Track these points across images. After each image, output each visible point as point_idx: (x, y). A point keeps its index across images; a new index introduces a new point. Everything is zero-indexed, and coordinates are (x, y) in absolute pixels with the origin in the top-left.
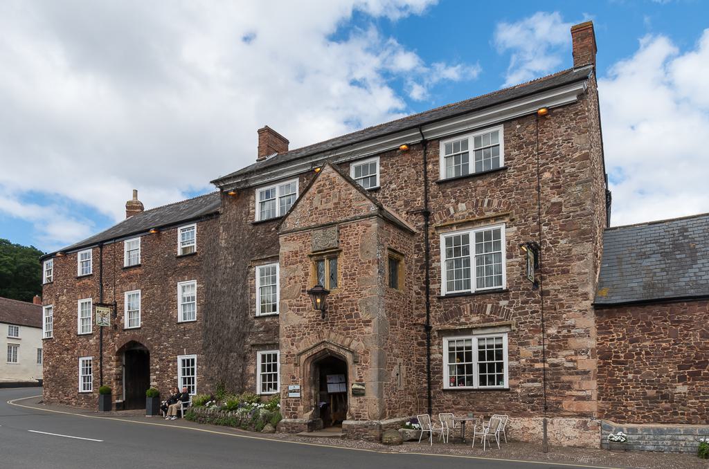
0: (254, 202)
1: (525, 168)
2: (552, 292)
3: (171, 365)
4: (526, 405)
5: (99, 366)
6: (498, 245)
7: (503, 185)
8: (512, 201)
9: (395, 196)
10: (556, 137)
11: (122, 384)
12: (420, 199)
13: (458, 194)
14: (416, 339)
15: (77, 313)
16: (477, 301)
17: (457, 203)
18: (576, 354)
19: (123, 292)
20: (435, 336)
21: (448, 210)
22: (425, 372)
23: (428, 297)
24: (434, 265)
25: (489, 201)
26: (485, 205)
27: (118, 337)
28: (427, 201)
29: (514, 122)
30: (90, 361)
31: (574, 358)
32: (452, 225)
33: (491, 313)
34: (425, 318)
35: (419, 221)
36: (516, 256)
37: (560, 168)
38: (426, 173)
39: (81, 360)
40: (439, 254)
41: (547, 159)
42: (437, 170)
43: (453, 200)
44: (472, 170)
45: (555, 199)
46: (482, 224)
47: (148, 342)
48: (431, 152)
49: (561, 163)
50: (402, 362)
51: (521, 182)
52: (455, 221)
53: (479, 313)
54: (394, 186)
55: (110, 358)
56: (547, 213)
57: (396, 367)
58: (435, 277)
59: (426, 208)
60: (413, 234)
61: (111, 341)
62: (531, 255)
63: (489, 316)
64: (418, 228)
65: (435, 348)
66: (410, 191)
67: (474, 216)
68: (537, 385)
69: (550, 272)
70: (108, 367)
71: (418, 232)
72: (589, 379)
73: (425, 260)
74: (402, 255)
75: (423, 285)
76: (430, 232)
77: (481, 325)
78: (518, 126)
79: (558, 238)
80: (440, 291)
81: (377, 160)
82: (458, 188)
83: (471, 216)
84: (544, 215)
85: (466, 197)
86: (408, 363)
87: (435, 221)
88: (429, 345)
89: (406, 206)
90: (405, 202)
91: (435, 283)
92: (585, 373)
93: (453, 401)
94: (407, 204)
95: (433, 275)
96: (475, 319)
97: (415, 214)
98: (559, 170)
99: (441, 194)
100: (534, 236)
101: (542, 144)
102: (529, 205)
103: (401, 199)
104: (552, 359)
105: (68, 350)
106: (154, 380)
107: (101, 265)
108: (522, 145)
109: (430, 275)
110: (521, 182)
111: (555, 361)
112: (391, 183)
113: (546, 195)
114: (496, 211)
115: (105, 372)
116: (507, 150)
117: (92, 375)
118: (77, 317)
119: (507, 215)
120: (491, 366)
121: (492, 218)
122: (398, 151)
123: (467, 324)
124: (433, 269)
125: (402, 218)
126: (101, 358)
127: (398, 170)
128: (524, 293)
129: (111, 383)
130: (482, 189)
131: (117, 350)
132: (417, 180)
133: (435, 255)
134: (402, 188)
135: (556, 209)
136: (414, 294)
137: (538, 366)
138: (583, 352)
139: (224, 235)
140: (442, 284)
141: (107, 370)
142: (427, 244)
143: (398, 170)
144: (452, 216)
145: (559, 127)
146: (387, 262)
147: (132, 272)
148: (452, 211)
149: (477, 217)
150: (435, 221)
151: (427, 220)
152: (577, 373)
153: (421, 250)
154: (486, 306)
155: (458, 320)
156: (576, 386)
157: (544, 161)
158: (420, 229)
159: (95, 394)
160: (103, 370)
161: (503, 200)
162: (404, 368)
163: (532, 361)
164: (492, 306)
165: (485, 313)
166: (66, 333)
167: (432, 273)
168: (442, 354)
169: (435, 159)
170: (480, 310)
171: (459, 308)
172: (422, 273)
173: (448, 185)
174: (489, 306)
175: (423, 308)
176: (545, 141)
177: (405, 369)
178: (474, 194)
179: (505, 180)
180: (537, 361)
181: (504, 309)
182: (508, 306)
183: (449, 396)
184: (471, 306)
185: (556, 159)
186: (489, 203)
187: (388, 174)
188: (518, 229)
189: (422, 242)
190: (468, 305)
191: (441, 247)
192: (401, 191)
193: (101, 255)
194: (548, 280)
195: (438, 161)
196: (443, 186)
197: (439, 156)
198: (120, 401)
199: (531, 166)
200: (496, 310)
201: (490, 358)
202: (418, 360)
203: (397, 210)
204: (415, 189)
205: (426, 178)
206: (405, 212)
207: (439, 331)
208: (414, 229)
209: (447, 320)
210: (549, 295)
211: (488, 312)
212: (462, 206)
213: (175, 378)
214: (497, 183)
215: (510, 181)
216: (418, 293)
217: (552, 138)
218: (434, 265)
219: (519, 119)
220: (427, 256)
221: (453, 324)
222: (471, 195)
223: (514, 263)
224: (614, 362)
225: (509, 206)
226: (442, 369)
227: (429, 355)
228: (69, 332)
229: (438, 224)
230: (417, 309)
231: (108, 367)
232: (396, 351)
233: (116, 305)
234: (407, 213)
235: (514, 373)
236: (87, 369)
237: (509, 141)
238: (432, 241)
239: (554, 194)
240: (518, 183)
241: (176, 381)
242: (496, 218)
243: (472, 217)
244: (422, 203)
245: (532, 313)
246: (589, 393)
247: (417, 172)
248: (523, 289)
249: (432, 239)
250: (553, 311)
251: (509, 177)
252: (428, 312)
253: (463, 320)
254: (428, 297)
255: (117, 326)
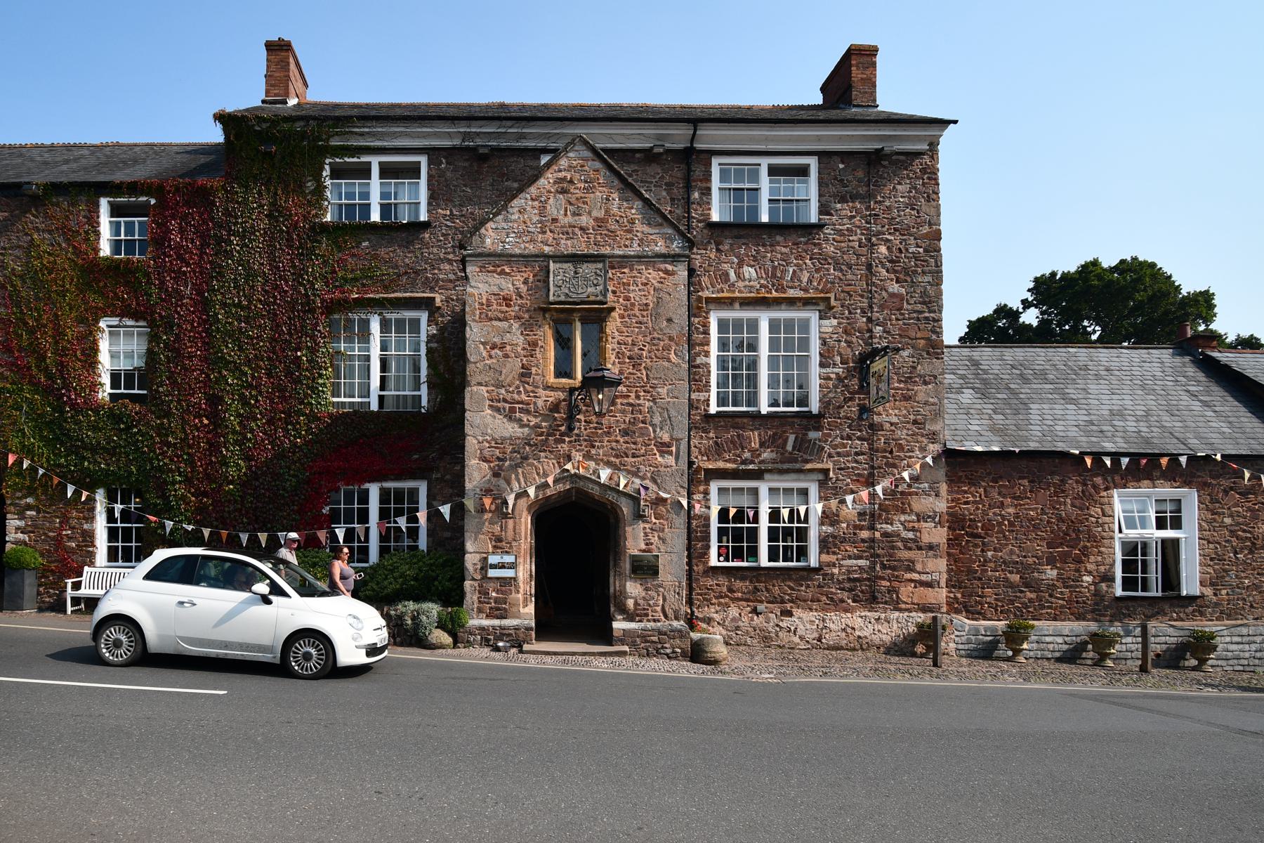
18: (919, 521)
31: (916, 525)
33: (794, 448)
46: (783, 307)
63: (791, 453)
68: (862, 562)
72: (935, 556)
77: (779, 466)
92: (931, 547)
104: (884, 526)
111: (889, 528)
137: (865, 534)
138: (929, 517)
149: (774, 294)
152: (920, 548)
156: (919, 567)
163: (856, 527)
164: (796, 438)
174: (792, 438)
181: (815, 443)
183: (723, 580)
211: (789, 448)
224: (967, 533)
235: (825, 545)
245: (857, 454)
246: (935, 576)
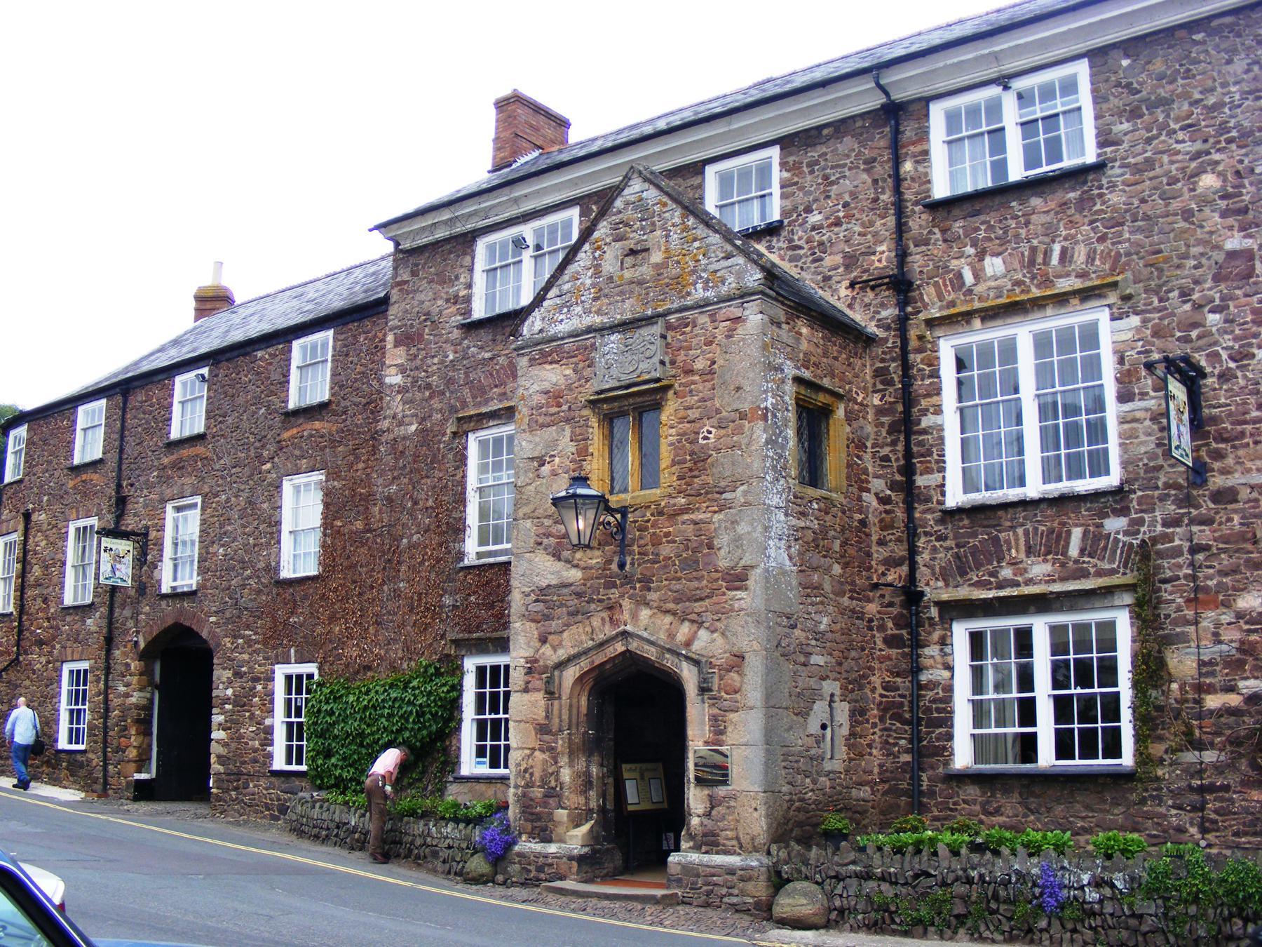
0: (471, 270)
1: (1149, 164)
2: (1244, 494)
3: (259, 687)
4: (1186, 817)
5: (102, 685)
6: (1093, 368)
7: (1098, 207)
8: (1122, 248)
9: (821, 244)
10: (1224, 85)
11: (151, 734)
12: (884, 248)
13: (982, 234)
14: (882, 628)
15: (64, 553)
16: (1046, 522)
17: (981, 255)
19: (164, 501)
20: (931, 619)
21: (959, 276)
22: (904, 722)
23: (910, 510)
24: (925, 422)
25: (1064, 252)
26: (1055, 260)
27: (147, 614)
28: (902, 255)
29: (1115, 54)
30: (85, 671)
32: (967, 316)
33: (1082, 551)
34: (905, 569)
35: (883, 305)
36: (1143, 395)
37: (1241, 162)
38: (898, 180)
39: (66, 668)
40: (938, 391)
41: (1205, 141)
42: (926, 174)
43: (970, 250)
44: (1016, 173)
45: (1234, 242)
46: (1049, 311)
47: (209, 626)
48: (909, 131)
49: (1243, 151)
50: (838, 692)
51: (1143, 201)
52: (977, 305)
53: (1048, 553)
54: (815, 218)
55: (128, 665)
56: (1217, 278)
57: (820, 708)
58: (930, 453)
59: (903, 274)
60: (870, 340)
61: (130, 624)
62: (1177, 390)
63: (1076, 562)
64: (881, 324)
65: (932, 651)
66: (858, 229)
67: (1028, 291)
69: (1236, 438)
70: (122, 689)
71: (881, 333)
73: (900, 408)
74: (839, 397)
75: (898, 477)
76: (913, 333)
78: (1125, 63)
79: (1251, 345)
80: (943, 494)
81: (774, 152)
82: (982, 218)
83: (1018, 290)
84: (1209, 284)
85: (1003, 241)
86: (854, 685)
87: (925, 306)
88: (917, 644)
89: (848, 267)
90: (846, 256)
91: (929, 471)
93: (983, 805)
94: (850, 261)
95: (923, 450)
96: (1039, 569)
97: (873, 288)
98: (1240, 167)
99: (938, 236)
100: (1187, 340)
101: (1191, 104)
102: (1167, 260)
103: (835, 249)
104: (1251, 682)
105: (40, 643)
106: (221, 727)
107: (122, 437)
108: (1139, 108)
109: (915, 449)
110: (1143, 201)
112: (808, 210)
113: (1211, 233)
114: (1083, 275)
115: (115, 701)
116: (1100, 121)
117: (86, 707)
118: (64, 564)
119: (1115, 285)
120: (1088, 702)
121: (1075, 293)
122: (825, 132)
123: (1018, 585)
124: (925, 432)
125: (839, 297)
126: (108, 670)
127: (826, 178)
128: (1168, 495)
129: (125, 728)
130: (1044, 219)
131: (142, 645)
132: (876, 200)
133: (928, 395)
134: (838, 223)
135: (1240, 266)
136: (875, 503)
139: (396, 356)
140: (948, 474)
141: (119, 696)
142: (906, 366)
143: (826, 178)
144: (970, 292)
145: (1229, 62)
146: (791, 415)
147: (185, 452)
148: (969, 278)
149: (1036, 292)
150: (925, 306)
151: (902, 305)
153: (890, 383)
154: (1069, 533)
155: (994, 574)
157: (1199, 145)
158: (888, 328)
159: (91, 756)
160: (111, 696)
161: (1100, 248)
162: (843, 711)
164: (1085, 534)
165: (1065, 553)
166: (39, 600)
167: (921, 444)
168: (950, 668)
169: (919, 148)
170: (1054, 545)
171: (996, 541)
172: (894, 443)
173: (956, 212)
174: (1077, 533)
175: (899, 540)
176: (1197, 96)
177: (847, 713)
178: (1023, 232)
179: (1101, 196)
180: (1211, 689)
181: (1116, 540)
182: (1126, 533)
183: (972, 791)
184: (1026, 533)
185: (1229, 141)
186: (1065, 256)
187: (802, 189)
188: (1144, 321)
189: (893, 360)
190: (1020, 531)
191: (942, 373)
192: (836, 229)
193: (124, 412)
194: (1230, 461)
195: (926, 153)
196: (941, 214)
197: (928, 140)
198: (144, 776)
199: (1165, 158)
200: (1095, 543)
201: (1085, 681)
202: (887, 687)
203: (827, 279)
204: (872, 224)
205: (897, 190)
206: (846, 283)
207: (942, 605)
208: (872, 328)
209: (963, 573)
210: (1236, 501)
211: (1074, 551)
212: (994, 265)
213: (268, 722)
214: (1082, 204)
215: (1115, 198)
216: (884, 500)
217: (1213, 90)
218: (925, 422)
219: (1131, 46)
220: (908, 398)
221: (981, 584)
222: (1017, 236)
223: (1138, 415)
225: (1116, 264)
226: (952, 712)
227: (916, 669)
228: (45, 600)
229: (935, 313)
230: (881, 543)
231: (122, 689)
232: (817, 659)
233: (146, 535)
234: (852, 285)
236: (77, 691)
237: (1106, 100)
238: (919, 357)
239: (1231, 228)
240: (1136, 203)
241: (269, 731)
242: (1086, 295)
243: (1023, 291)
244: (888, 260)
247: (875, 181)
248: (1167, 486)
249: (920, 350)
250: (1249, 546)
251: (1112, 186)
252: (913, 552)
253: (1006, 573)
254: (910, 510)
255: (144, 586)
